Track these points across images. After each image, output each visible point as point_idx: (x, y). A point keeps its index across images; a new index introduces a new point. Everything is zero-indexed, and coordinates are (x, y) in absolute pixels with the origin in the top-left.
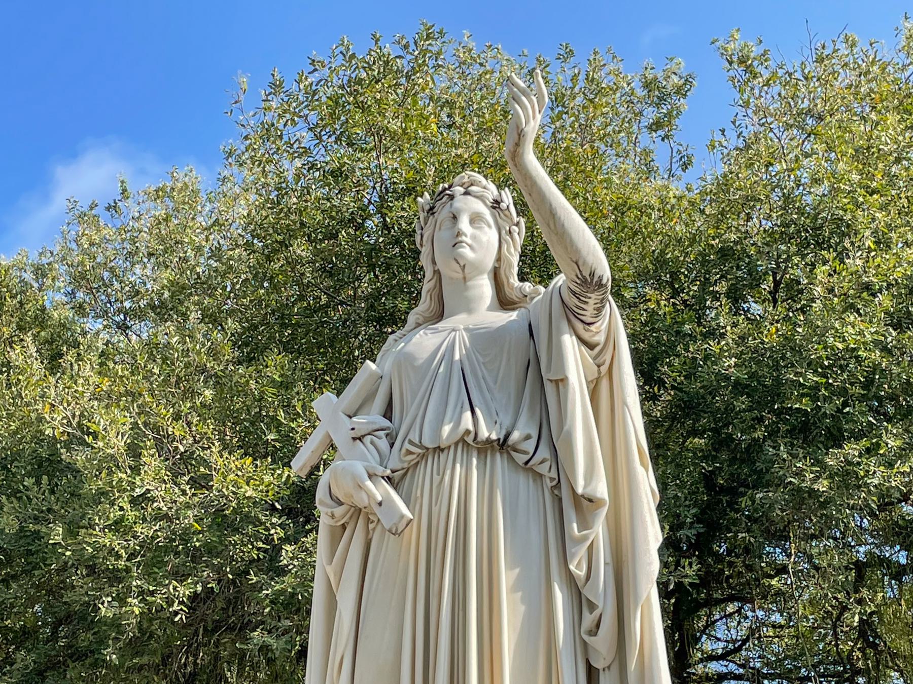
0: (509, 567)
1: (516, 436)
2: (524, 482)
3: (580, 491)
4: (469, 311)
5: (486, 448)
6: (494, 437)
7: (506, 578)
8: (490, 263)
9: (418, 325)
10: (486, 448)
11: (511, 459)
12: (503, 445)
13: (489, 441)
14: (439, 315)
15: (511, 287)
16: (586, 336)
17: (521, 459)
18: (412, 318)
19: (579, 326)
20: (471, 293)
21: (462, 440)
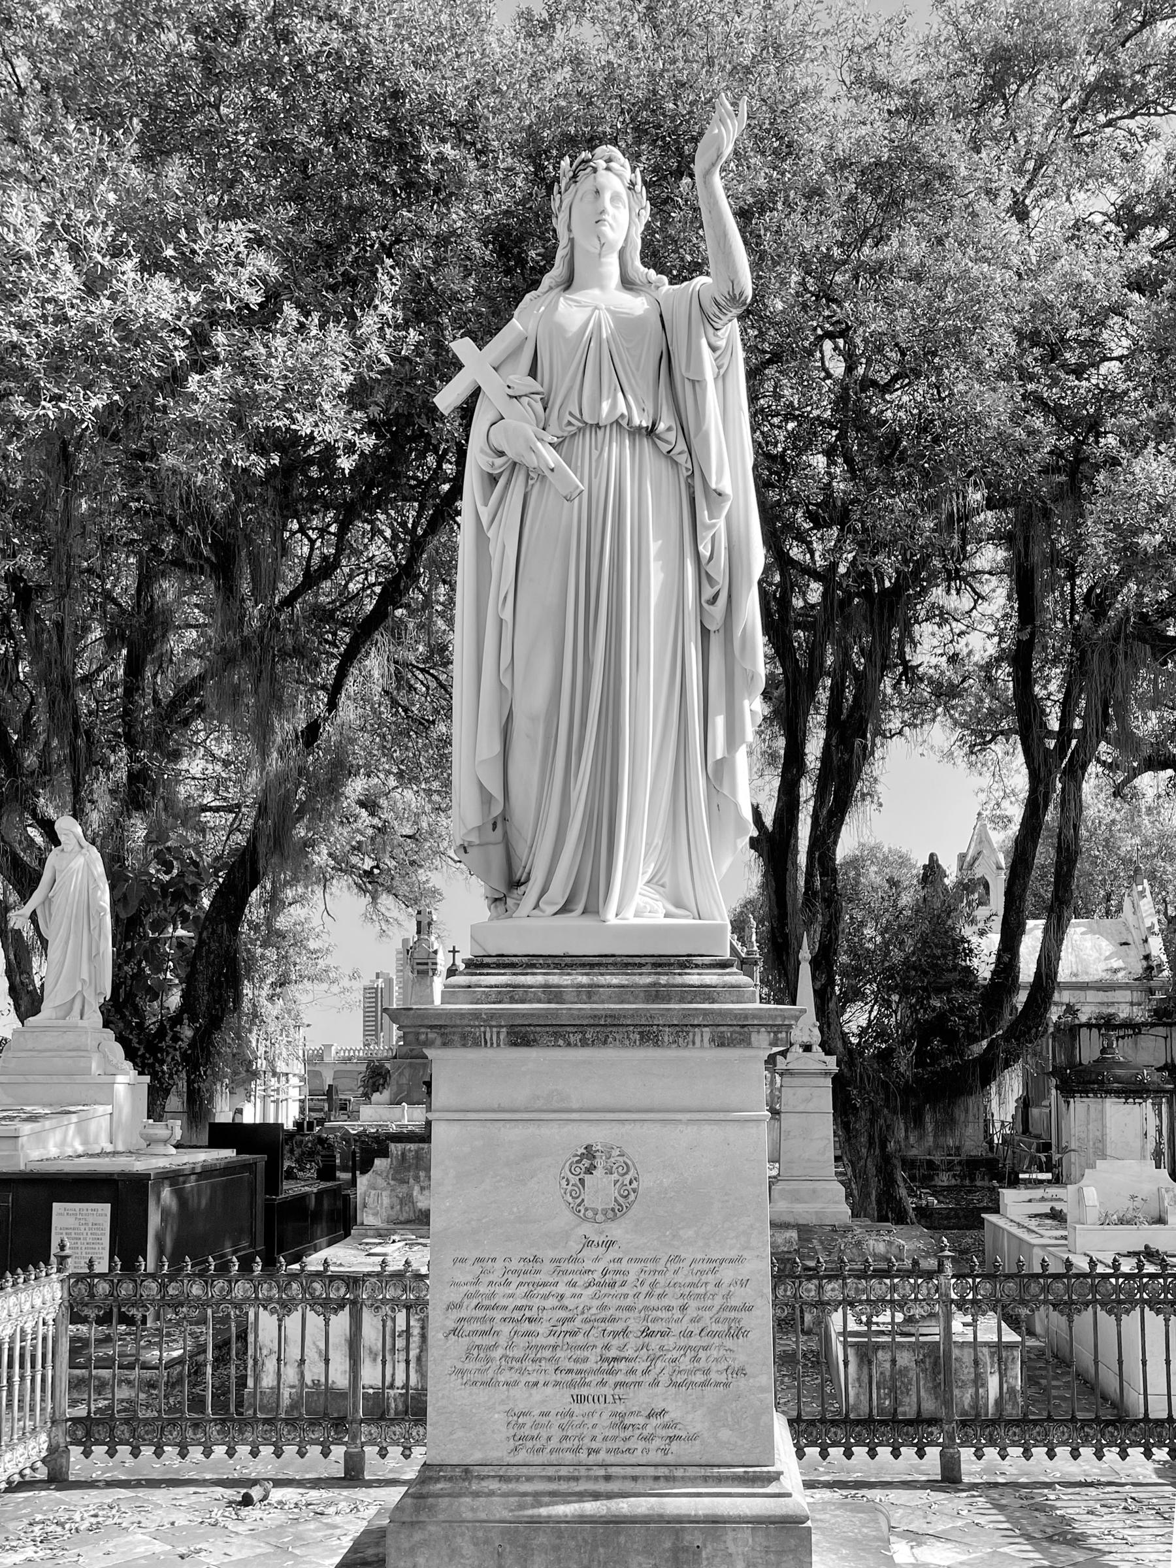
0: (655, 540)
1: (662, 427)
2: (664, 465)
3: (713, 486)
4: (602, 287)
5: (636, 432)
6: (644, 424)
7: (654, 547)
8: (620, 244)
9: (551, 288)
10: (636, 432)
11: (654, 443)
12: (651, 432)
13: (640, 428)
14: (568, 283)
15: (637, 271)
16: (713, 340)
17: (665, 448)
18: (547, 280)
19: (710, 330)
20: (604, 270)
21: (617, 421)
